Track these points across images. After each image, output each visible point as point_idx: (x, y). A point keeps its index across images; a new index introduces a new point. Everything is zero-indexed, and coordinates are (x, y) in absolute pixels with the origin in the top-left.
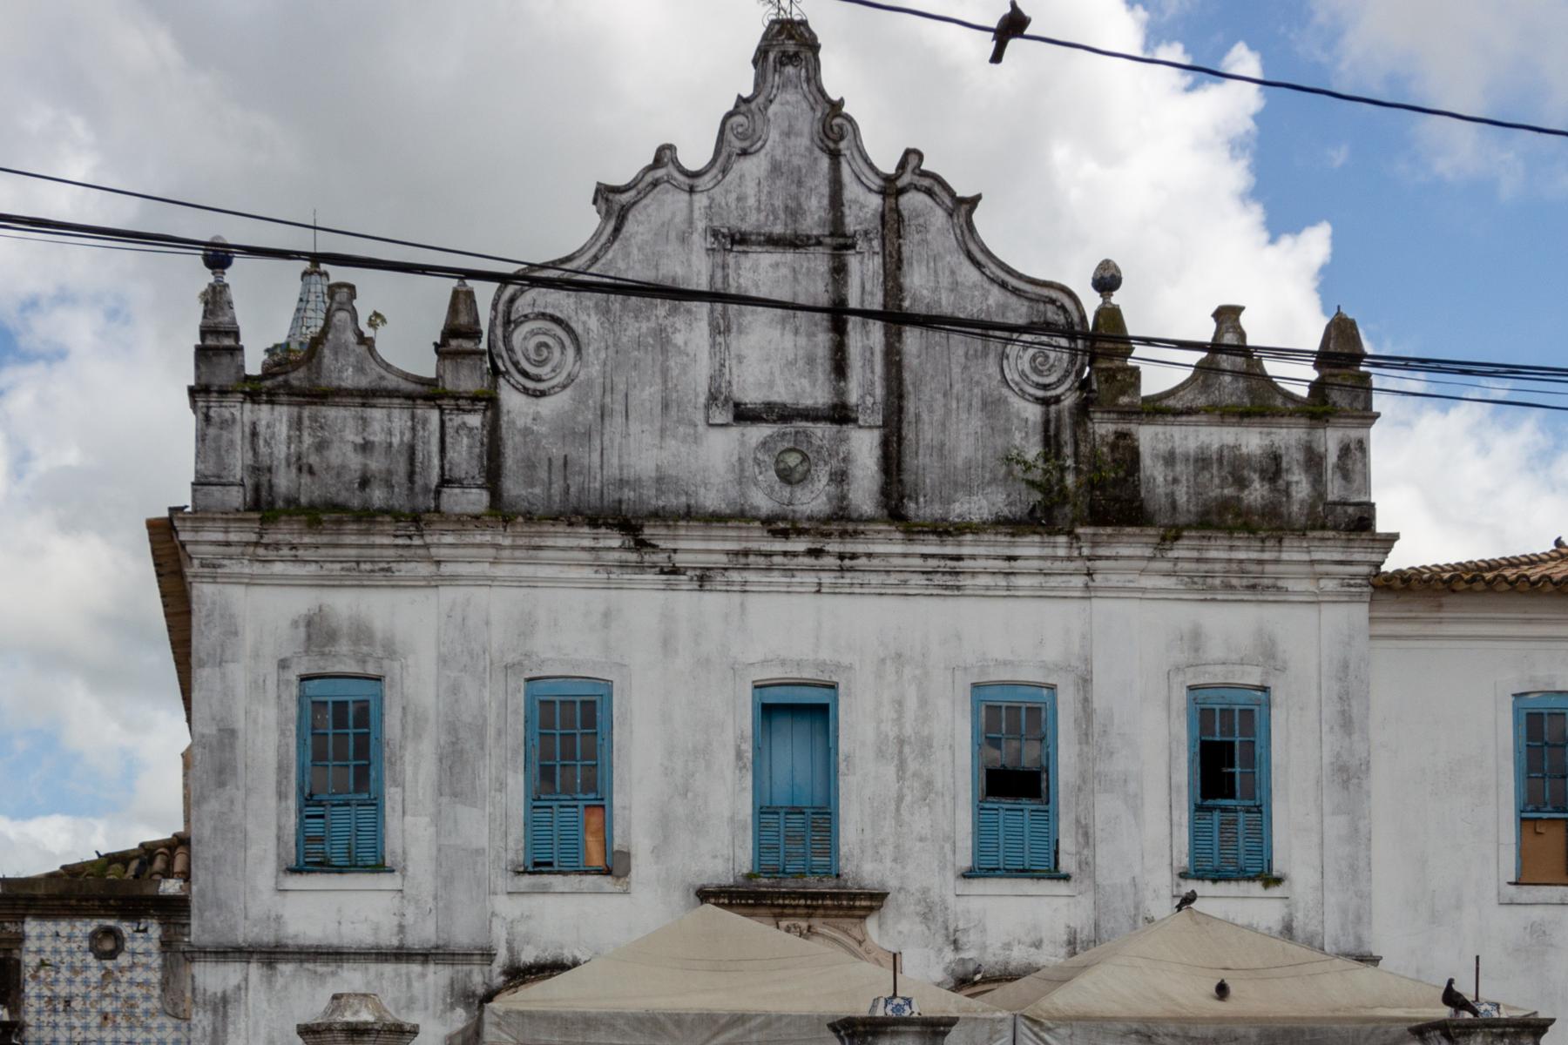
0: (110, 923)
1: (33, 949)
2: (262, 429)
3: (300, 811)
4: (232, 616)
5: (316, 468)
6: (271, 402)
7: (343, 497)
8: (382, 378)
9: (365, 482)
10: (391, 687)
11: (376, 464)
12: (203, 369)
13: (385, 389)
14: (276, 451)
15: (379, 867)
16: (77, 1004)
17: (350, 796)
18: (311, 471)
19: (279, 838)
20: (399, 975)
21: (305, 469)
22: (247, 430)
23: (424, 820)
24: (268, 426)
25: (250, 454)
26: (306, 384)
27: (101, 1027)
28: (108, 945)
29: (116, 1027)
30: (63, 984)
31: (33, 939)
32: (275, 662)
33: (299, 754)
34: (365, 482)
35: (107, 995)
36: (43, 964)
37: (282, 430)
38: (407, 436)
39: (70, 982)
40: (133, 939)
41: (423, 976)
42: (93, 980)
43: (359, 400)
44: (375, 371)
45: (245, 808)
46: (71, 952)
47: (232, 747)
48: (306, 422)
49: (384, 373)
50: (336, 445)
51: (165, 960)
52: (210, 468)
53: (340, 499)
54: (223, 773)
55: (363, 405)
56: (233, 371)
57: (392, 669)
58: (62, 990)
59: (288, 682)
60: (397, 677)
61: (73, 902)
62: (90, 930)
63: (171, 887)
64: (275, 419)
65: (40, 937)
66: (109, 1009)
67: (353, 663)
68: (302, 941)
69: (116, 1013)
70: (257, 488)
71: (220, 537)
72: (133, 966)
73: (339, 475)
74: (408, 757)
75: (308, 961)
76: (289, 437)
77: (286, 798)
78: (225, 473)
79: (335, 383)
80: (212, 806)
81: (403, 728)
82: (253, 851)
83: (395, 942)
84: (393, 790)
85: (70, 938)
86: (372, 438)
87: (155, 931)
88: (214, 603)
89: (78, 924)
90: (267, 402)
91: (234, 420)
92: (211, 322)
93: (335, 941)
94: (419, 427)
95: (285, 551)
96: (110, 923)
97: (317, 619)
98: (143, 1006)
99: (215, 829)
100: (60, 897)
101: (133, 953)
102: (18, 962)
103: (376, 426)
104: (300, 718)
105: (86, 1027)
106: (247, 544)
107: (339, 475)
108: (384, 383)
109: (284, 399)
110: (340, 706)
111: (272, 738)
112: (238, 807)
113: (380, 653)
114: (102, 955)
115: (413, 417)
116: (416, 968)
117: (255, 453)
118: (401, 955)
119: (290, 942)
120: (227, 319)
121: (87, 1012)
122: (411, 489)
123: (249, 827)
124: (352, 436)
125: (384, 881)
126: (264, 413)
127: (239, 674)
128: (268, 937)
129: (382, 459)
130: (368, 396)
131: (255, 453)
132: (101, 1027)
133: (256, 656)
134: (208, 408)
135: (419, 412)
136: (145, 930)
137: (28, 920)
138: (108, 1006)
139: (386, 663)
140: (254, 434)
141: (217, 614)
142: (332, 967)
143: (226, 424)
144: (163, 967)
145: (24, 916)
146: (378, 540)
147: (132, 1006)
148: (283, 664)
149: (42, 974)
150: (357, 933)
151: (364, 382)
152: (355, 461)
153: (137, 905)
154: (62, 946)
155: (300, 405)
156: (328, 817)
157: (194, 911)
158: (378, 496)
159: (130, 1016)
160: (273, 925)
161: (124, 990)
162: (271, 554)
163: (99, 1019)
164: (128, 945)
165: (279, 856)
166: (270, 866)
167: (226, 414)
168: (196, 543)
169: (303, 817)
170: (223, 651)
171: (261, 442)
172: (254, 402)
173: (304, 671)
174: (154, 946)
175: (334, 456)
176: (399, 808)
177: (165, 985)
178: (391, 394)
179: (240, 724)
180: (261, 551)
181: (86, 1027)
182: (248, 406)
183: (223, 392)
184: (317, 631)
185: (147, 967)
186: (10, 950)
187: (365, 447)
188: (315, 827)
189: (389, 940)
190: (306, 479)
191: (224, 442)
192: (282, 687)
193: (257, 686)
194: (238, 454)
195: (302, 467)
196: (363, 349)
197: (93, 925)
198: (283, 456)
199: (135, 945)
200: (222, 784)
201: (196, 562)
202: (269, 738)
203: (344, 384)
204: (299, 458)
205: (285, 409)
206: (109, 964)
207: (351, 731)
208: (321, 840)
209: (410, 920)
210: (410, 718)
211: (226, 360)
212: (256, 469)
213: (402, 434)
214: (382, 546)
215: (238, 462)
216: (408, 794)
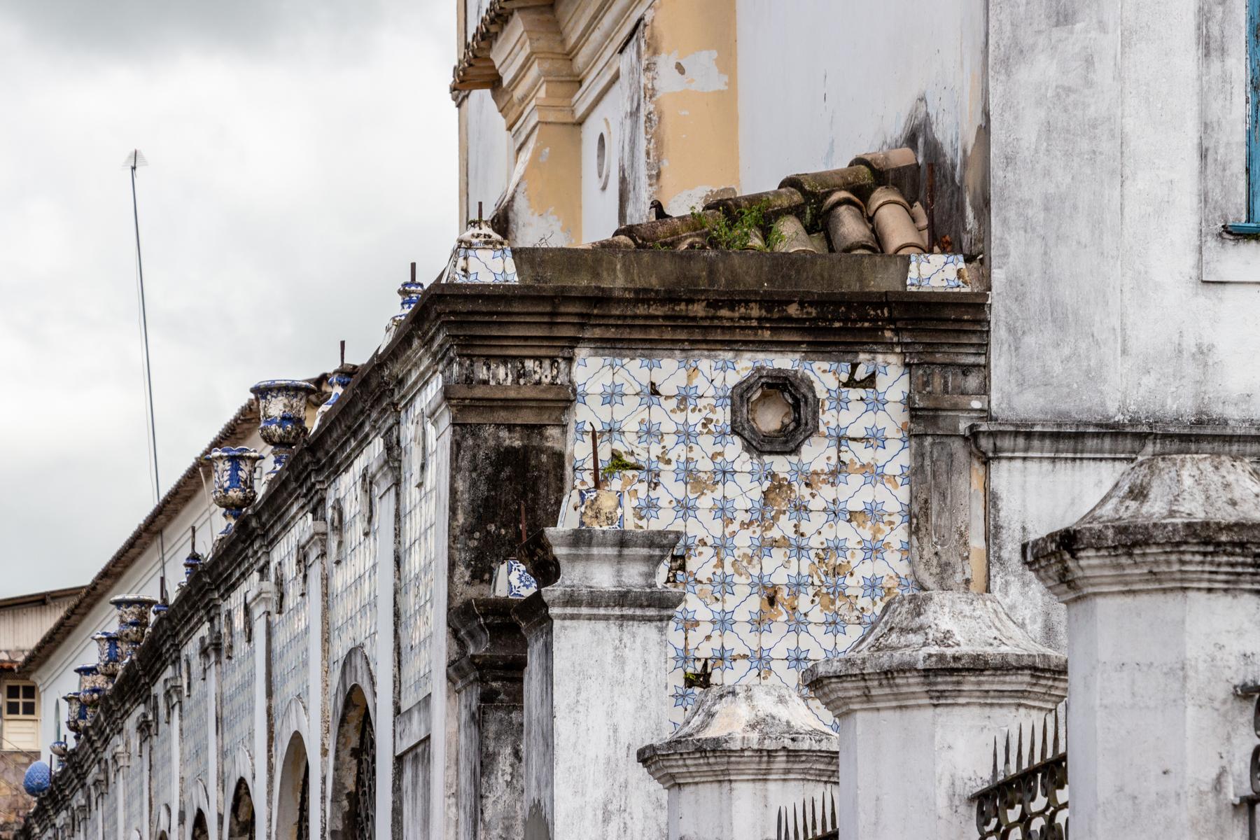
0: (784, 362)
19: (1203, 155)
27: (759, 623)
28: (770, 419)
29: (798, 624)
31: (594, 401)
35: (775, 543)
40: (841, 404)
42: (742, 503)
45: (1119, 77)
51: (919, 455)
61: (698, 309)
62: (733, 379)
63: (935, 273)
65: (611, 397)
66: (780, 578)
69: (797, 587)
72: (838, 471)
77: (1223, 51)
80: (1041, 70)
87: (894, 381)
89: (705, 364)
96: (784, 362)
98: (866, 570)
99: (1048, 128)
100: (670, 298)
101: (841, 439)
102: (559, 459)
105: (724, 623)
112: (1104, 74)
114: (759, 445)
119: (1233, 413)
121: (726, 585)
123: (1130, 125)
128: (1176, 401)
132: (759, 623)
136: (870, 381)
137: (582, 353)
138: (778, 569)
144: (916, 473)
145: (575, 342)
147: (836, 571)
153: (850, 319)
154: (665, 417)
157: (999, 333)
159: (832, 594)
160: (1191, 370)
161: (818, 531)
163: (756, 603)
164: (828, 418)
165: (1204, 198)
166: (1184, 221)
174: (892, 420)
177: (917, 520)
181: (724, 623)
185: (873, 473)
197: (744, 365)
199: (845, 418)
206: (780, 465)
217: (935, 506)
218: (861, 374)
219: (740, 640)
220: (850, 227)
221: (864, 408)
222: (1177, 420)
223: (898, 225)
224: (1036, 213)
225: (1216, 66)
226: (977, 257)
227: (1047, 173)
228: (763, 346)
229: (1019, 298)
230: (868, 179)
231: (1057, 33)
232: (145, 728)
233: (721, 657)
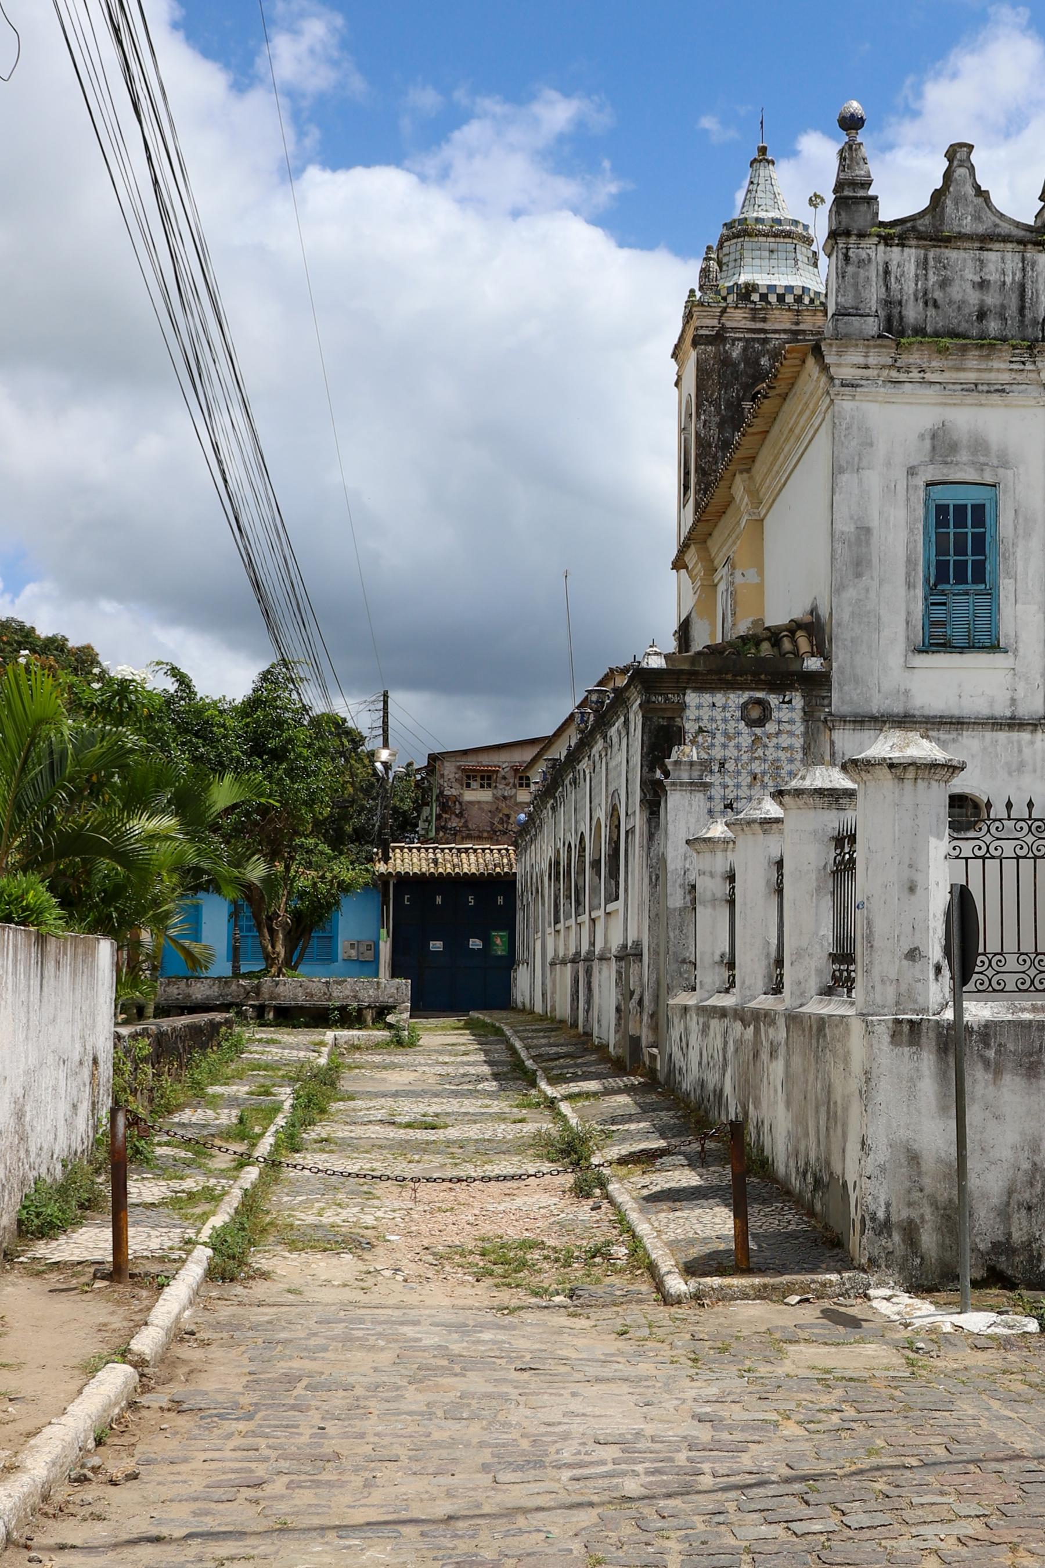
0: (760, 695)
1: (692, 717)
2: (893, 268)
3: (926, 599)
4: (867, 429)
5: (940, 302)
6: (903, 246)
7: (963, 327)
8: (996, 225)
9: (982, 315)
10: (1005, 492)
11: (992, 300)
12: (843, 214)
13: (999, 235)
14: (906, 288)
15: (994, 647)
16: (730, 766)
17: (968, 587)
18: (936, 305)
19: (907, 623)
20: (1010, 742)
21: (930, 303)
22: (881, 269)
23: (1036, 607)
24: (899, 266)
25: (883, 289)
26: (931, 230)
27: (750, 786)
28: (755, 713)
30: (718, 748)
31: (693, 709)
32: (905, 470)
33: (925, 550)
34: (982, 315)
35: (756, 758)
36: (701, 730)
37: (911, 269)
38: (1019, 276)
39: (724, 746)
40: (779, 709)
41: (1032, 743)
42: (744, 744)
43: (977, 245)
44: (990, 219)
45: (878, 596)
46: (725, 721)
47: (868, 543)
48: (931, 263)
49: (998, 221)
50: (957, 282)
51: (807, 728)
52: (848, 301)
53: (961, 329)
54: (860, 565)
55: (981, 249)
56: (869, 217)
57: (1006, 476)
58: (718, 753)
59: (916, 487)
60: (1011, 484)
61: (729, 677)
62: (742, 701)
63: (813, 664)
64: (905, 260)
65: (699, 707)
66: (758, 771)
67: (972, 471)
68: (927, 712)
69: (764, 773)
70: (889, 319)
71: (861, 360)
72: (779, 733)
73: (959, 308)
74: (1020, 552)
75: (933, 729)
76: (917, 276)
77: (915, 587)
78: (861, 306)
79: (956, 229)
81: (1015, 529)
82: (885, 633)
83: (1008, 714)
84: (1007, 581)
85: (724, 708)
86: (988, 277)
87: (798, 701)
88: (853, 417)
89: (732, 696)
90: (897, 245)
91: (870, 260)
92: (848, 175)
93: (956, 712)
94: (1028, 269)
95: (915, 375)
96: (760, 695)
97: (941, 433)
98: (788, 767)
99: (853, 613)
101: (779, 722)
103: (991, 267)
104: (926, 519)
105: (738, 786)
106: (883, 367)
107: (959, 308)
108: (998, 230)
109: (913, 242)
110: (960, 509)
111: (903, 535)
112: (872, 595)
113: (995, 462)
114: (751, 723)
115: (1023, 260)
116: (1025, 736)
117: (888, 289)
118: (1014, 724)
119: (917, 713)
120: (862, 173)
121: (739, 773)
122: (1022, 322)
124: (970, 275)
125: (998, 659)
126: (895, 253)
127: (873, 479)
128: (898, 708)
129: (997, 295)
130: (986, 240)
131: (888, 289)
132: (750, 786)
133: (888, 464)
134: (848, 249)
135: (1028, 255)
136: (790, 702)
137: (688, 691)
138: (757, 767)
139: (1001, 471)
140: (887, 272)
141: (855, 427)
142: (954, 735)
143: (862, 263)
144: (806, 734)
145: (686, 688)
146: (996, 364)
147: (778, 768)
148: (912, 471)
149: (700, 739)
150: (975, 706)
151: (981, 229)
152: (973, 297)
154: (717, 714)
155: (926, 248)
156: (950, 605)
157: (835, 685)
158: (993, 326)
160: (902, 698)
161: (771, 753)
162: (903, 377)
163: (749, 779)
164: (775, 715)
165: (908, 638)
167: (864, 256)
168: (839, 365)
169: (929, 605)
170: (860, 459)
171: (893, 280)
172: (886, 245)
173: (930, 478)
174: (797, 716)
175: (956, 292)
176: (1012, 597)
178: (1006, 239)
179: (875, 523)
180: (894, 374)
181: (738, 786)
182: (881, 248)
183: (862, 235)
184: (941, 444)
186: (674, 718)
187: (982, 285)
188: (938, 613)
189: (1003, 710)
190: (931, 312)
191: (861, 280)
192: (911, 492)
193: (889, 490)
194: (874, 290)
195: (928, 301)
196: (981, 200)
197: (746, 696)
198: (911, 291)
199: (781, 714)
200: (859, 575)
201: (837, 382)
202: (900, 537)
203: (963, 231)
204: (925, 294)
205: (913, 250)
206: (758, 731)
207: (969, 530)
208: (943, 624)
209: (1020, 694)
210: (1021, 520)
211: (863, 208)
212: (888, 303)
213: (1014, 274)
214: (998, 370)
215: (873, 295)
216: (1019, 584)
217: (812, 746)
218: (787, 699)
219: (743, 792)
220: (787, 645)
221: (789, 711)
222: (897, 716)
223: (804, 644)
224: (848, 643)
225: (912, 592)
226: (827, 658)
227: (852, 629)
228: (753, 689)
229: (842, 673)
230: (795, 627)
231: (856, 580)
232: (554, 809)
233: (737, 798)
